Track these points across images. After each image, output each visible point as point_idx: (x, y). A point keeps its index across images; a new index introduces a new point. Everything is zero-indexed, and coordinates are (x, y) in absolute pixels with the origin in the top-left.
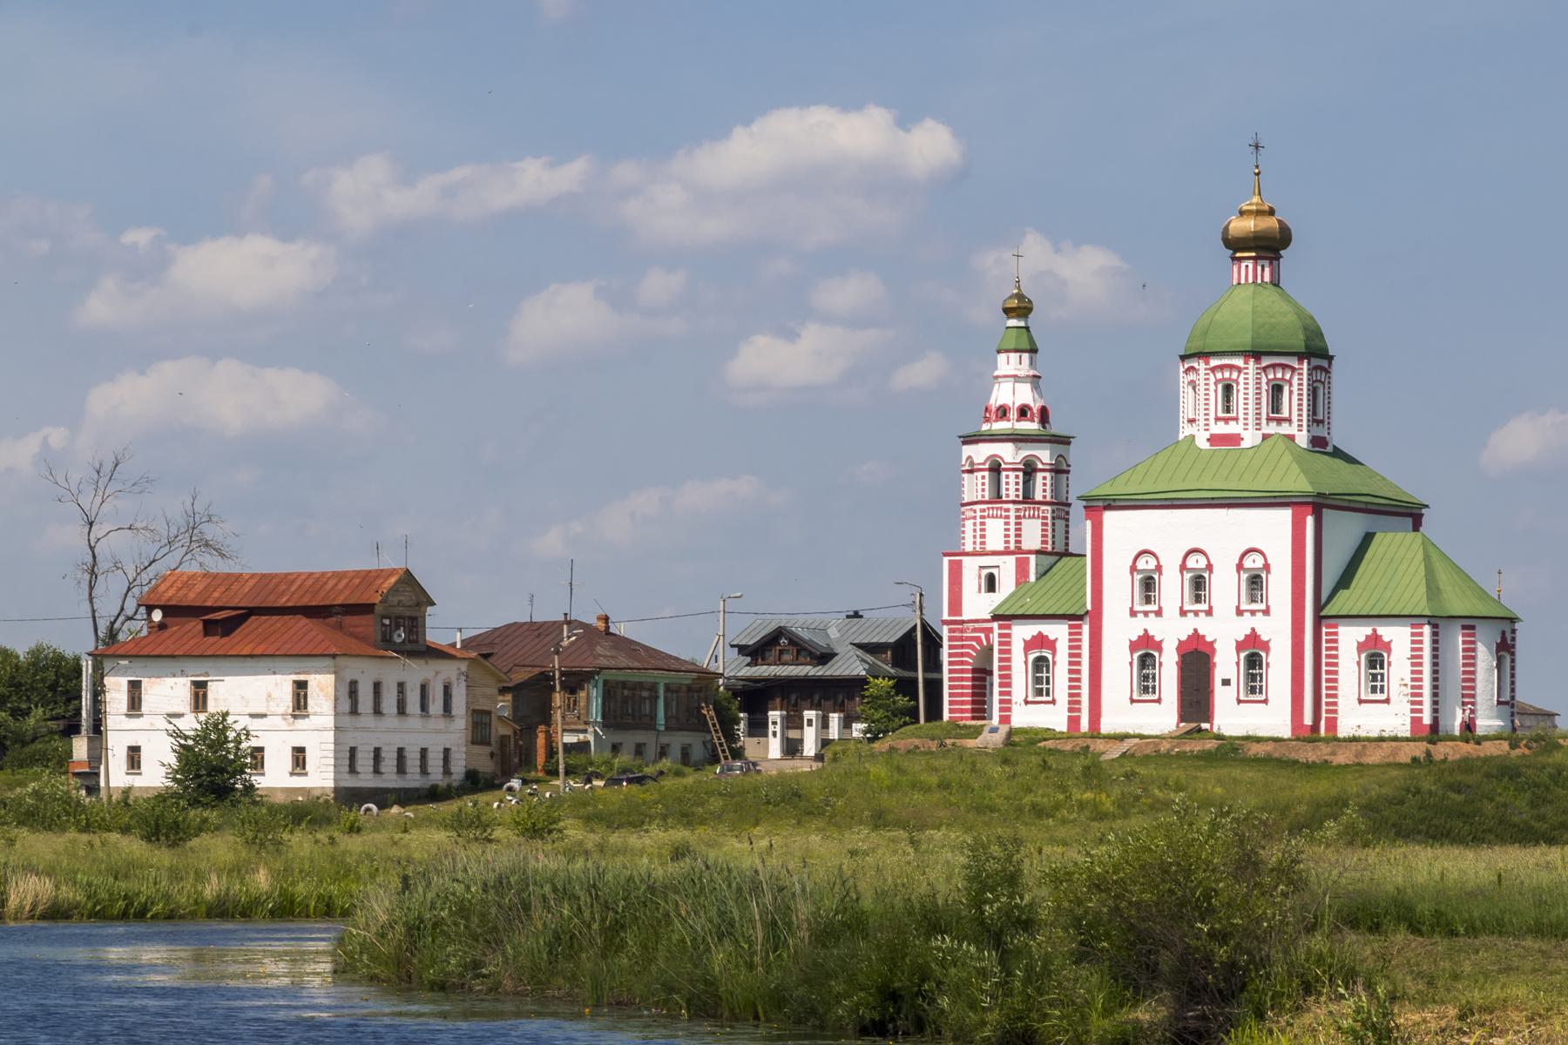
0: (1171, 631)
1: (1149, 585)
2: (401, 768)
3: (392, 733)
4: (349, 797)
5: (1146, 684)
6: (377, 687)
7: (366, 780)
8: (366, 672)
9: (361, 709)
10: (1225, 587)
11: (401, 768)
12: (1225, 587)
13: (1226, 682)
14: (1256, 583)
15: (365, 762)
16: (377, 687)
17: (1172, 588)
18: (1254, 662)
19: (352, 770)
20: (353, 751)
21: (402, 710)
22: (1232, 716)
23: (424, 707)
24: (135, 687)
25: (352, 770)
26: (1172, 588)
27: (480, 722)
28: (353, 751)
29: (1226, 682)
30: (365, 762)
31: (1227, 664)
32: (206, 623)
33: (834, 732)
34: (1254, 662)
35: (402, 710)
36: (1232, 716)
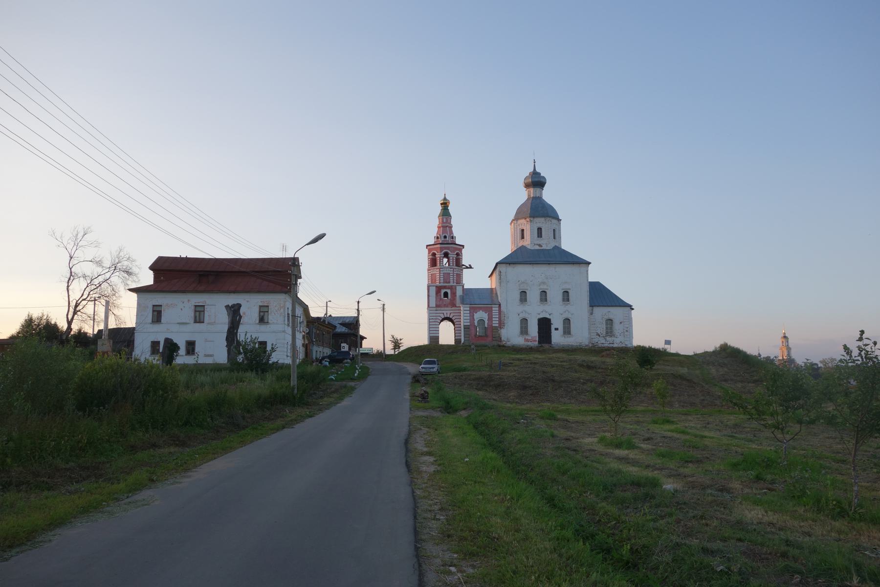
0: (534, 311)
1: (524, 296)
5: (524, 330)
10: (555, 295)
12: (555, 295)
13: (556, 329)
17: (533, 296)
18: (567, 322)
26: (533, 296)
29: (556, 329)
31: (557, 323)
34: (567, 322)
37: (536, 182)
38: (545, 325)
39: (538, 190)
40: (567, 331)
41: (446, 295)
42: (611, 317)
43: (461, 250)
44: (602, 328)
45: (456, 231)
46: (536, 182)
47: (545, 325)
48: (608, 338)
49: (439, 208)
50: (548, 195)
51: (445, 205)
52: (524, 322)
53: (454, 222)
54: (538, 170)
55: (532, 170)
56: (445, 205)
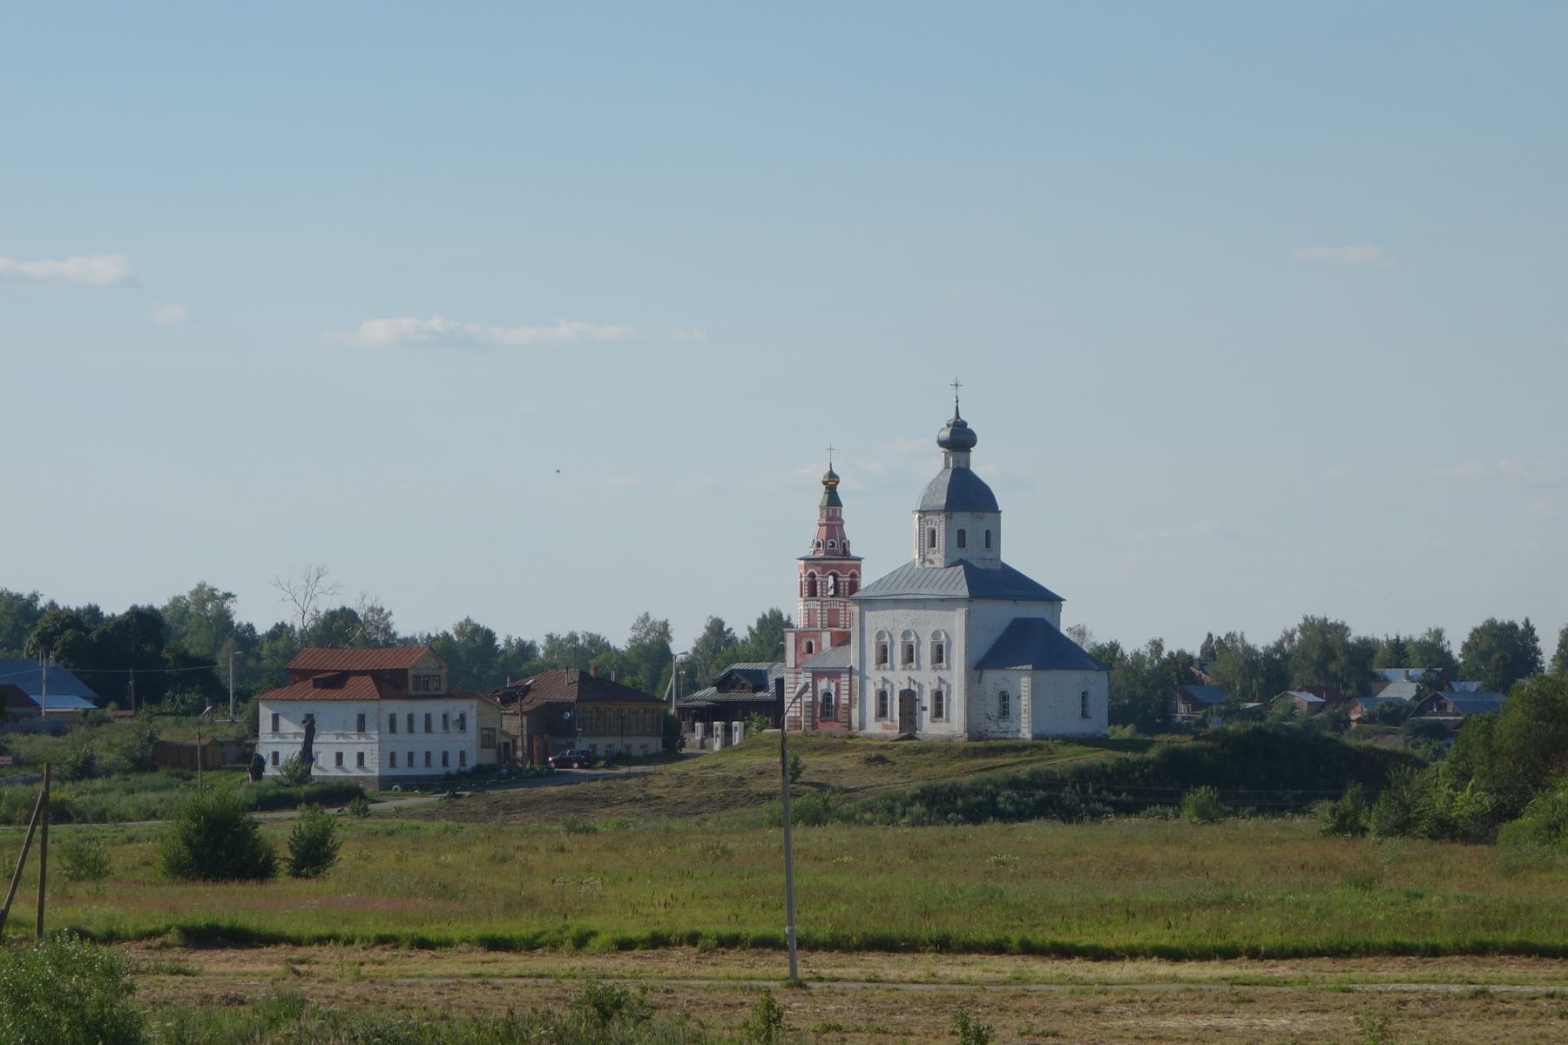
2: (428, 763)
3: (420, 743)
4: (386, 783)
5: (882, 712)
6: (410, 718)
7: (402, 769)
8: (401, 708)
9: (416, 728)
11: (428, 763)
14: (939, 655)
15: (402, 760)
16: (410, 718)
19: (393, 765)
20: (393, 756)
21: (428, 729)
22: (929, 728)
23: (446, 726)
24: (275, 718)
25: (393, 765)
27: (488, 738)
28: (393, 756)
30: (402, 760)
32: (315, 681)
33: (737, 738)
34: (938, 696)
35: (428, 729)
36: (929, 728)
37: (960, 440)
38: (909, 699)
39: (963, 455)
40: (938, 713)
41: (810, 645)
42: (1005, 687)
43: (858, 567)
44: (994, 707)
45: (850, 531)
46: (960, 440)
47: (909, 699)
48: (1002, 724)
49: (820, 494)
50: (981, 464)
51: (831, 482)
52: (882, 696)
53: (846, 513)
54: (963, 417)
55: (952, 415)
56: (831, 482)
